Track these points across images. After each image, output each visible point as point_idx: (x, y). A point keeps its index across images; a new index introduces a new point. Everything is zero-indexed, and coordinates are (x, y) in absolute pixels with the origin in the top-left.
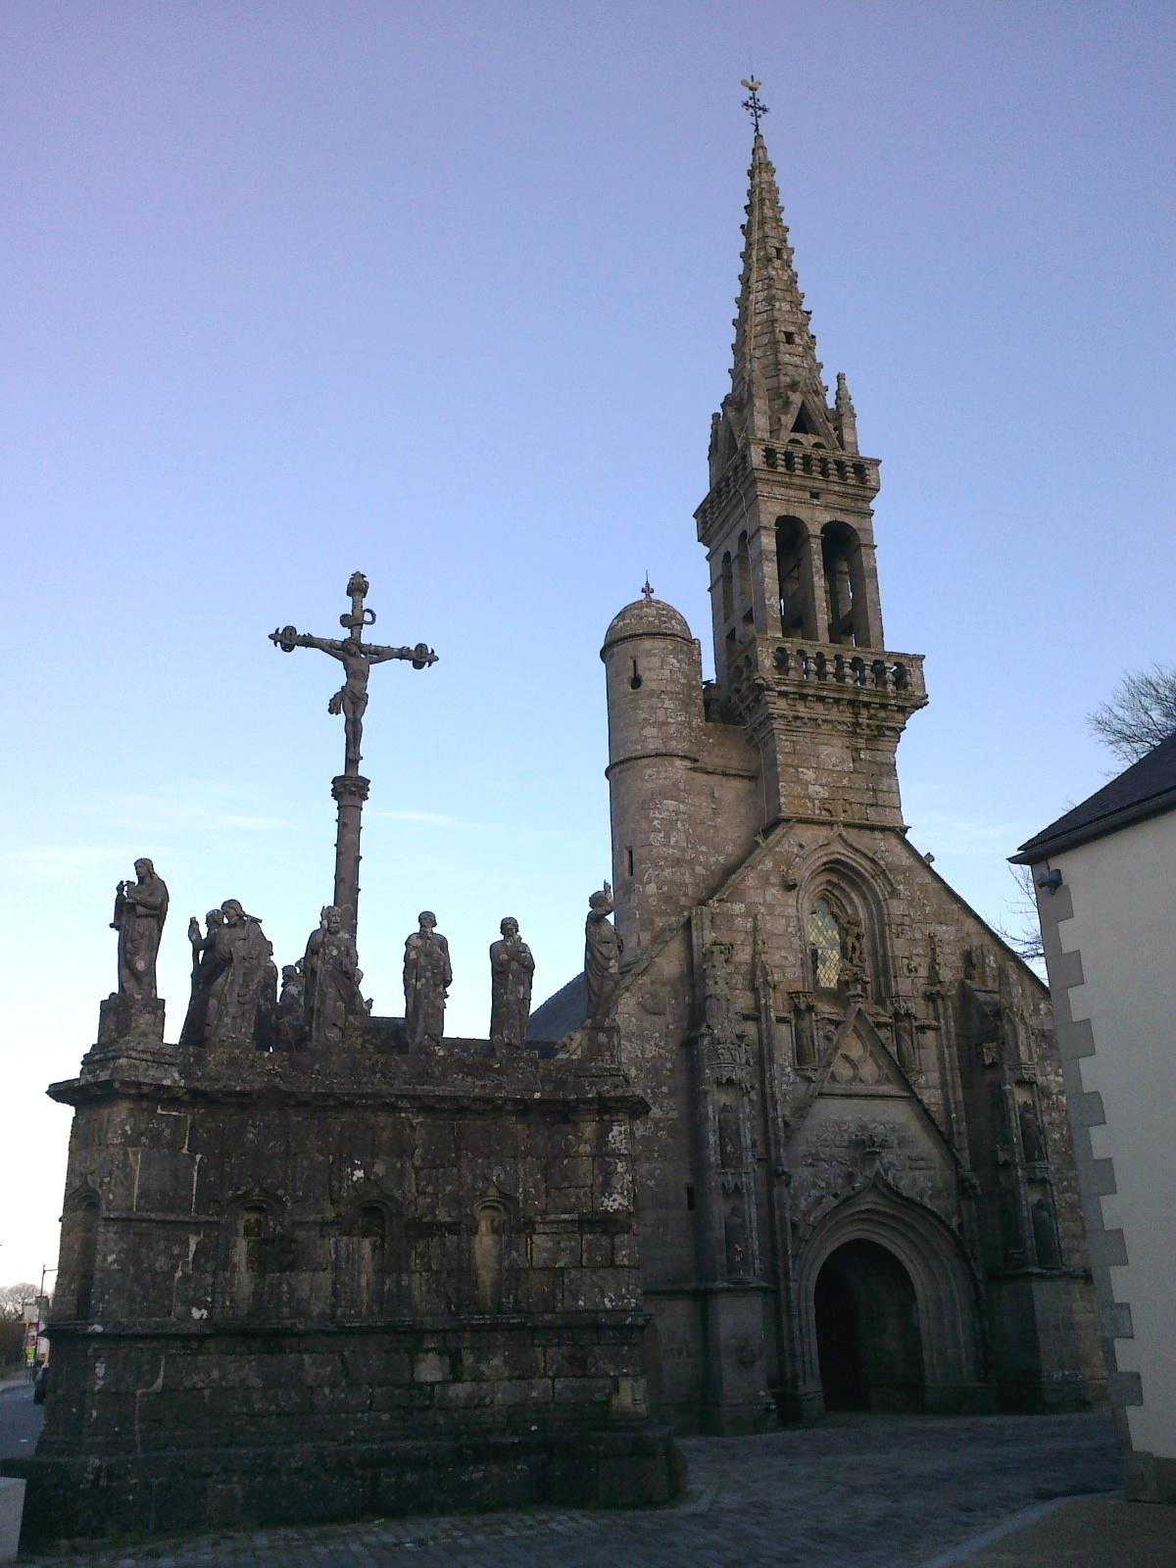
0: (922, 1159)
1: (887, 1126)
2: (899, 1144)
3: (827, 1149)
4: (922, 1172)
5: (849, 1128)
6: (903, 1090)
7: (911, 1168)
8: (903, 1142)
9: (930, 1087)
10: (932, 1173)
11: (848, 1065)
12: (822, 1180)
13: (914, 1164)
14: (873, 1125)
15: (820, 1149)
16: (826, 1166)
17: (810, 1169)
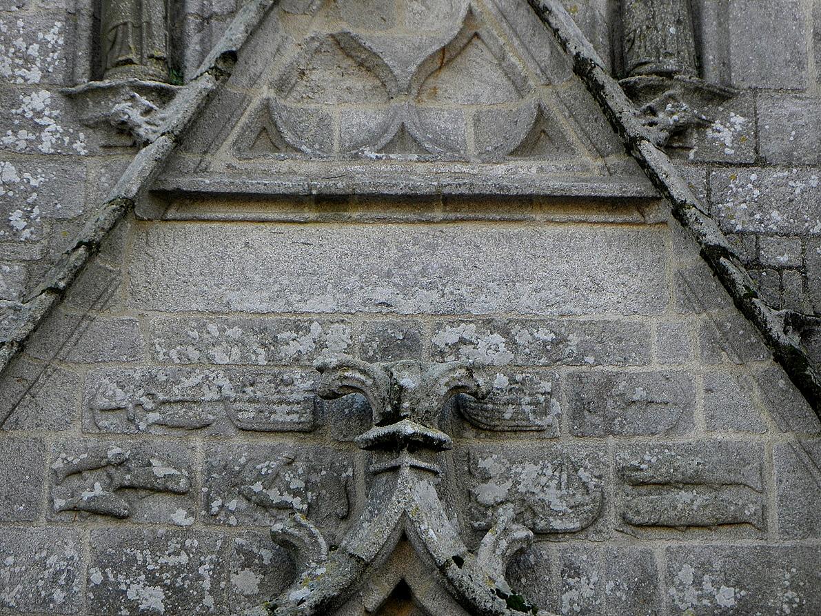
0: (689, 483)
1: (523, 337)
2: (576, 415)
3: (197, 441)
4: (695, 541)
5: (321, 345)
6: (610, 171)
7: (634, 525)
8: (594, 406)
9: (761, 162)
10: (747, 541)
11: (360, 82)
12: (153, 580)
13: (644, 504)
14: (450, 335)
15: (160, 440)
16: (180, 516)
17: (93, 531)
